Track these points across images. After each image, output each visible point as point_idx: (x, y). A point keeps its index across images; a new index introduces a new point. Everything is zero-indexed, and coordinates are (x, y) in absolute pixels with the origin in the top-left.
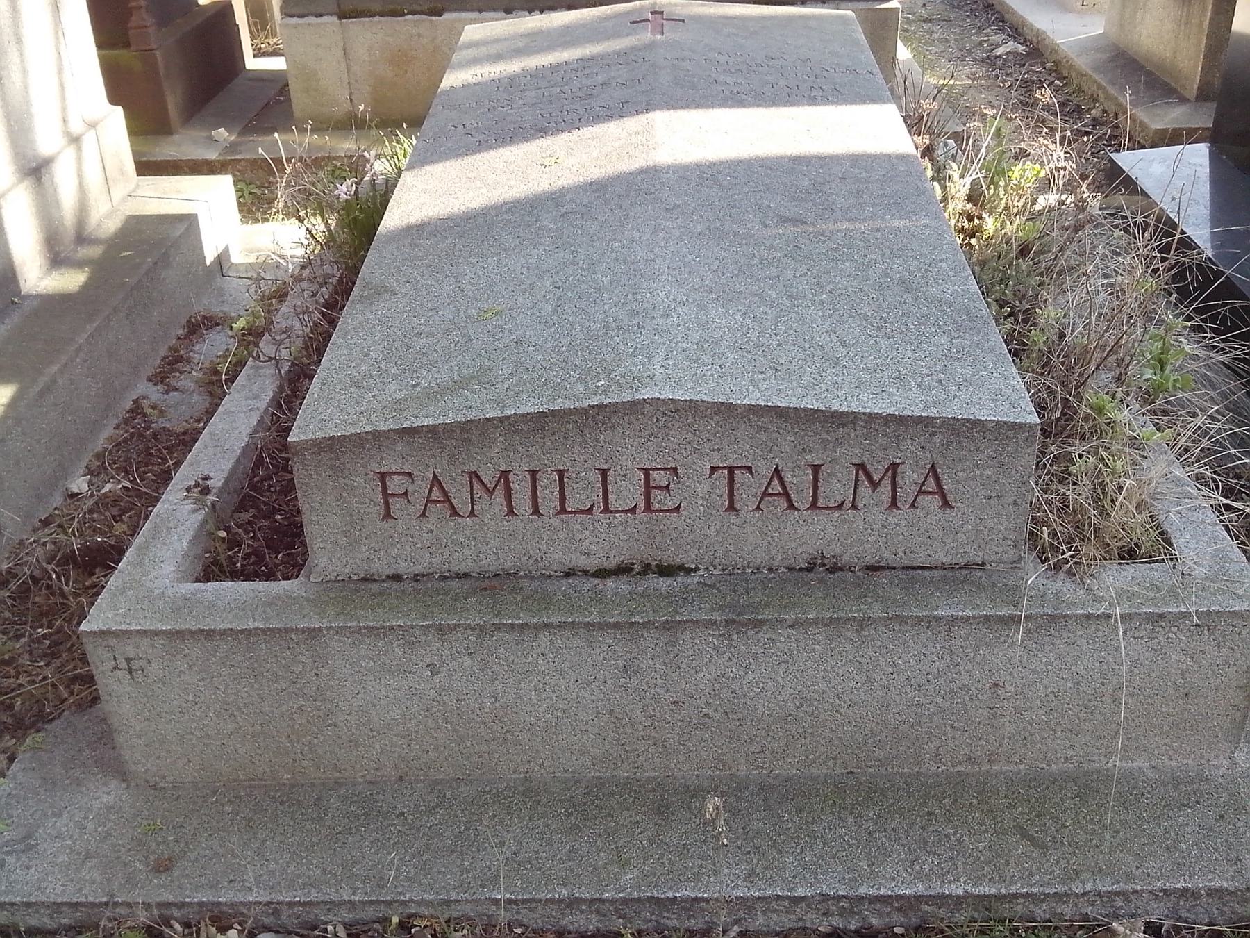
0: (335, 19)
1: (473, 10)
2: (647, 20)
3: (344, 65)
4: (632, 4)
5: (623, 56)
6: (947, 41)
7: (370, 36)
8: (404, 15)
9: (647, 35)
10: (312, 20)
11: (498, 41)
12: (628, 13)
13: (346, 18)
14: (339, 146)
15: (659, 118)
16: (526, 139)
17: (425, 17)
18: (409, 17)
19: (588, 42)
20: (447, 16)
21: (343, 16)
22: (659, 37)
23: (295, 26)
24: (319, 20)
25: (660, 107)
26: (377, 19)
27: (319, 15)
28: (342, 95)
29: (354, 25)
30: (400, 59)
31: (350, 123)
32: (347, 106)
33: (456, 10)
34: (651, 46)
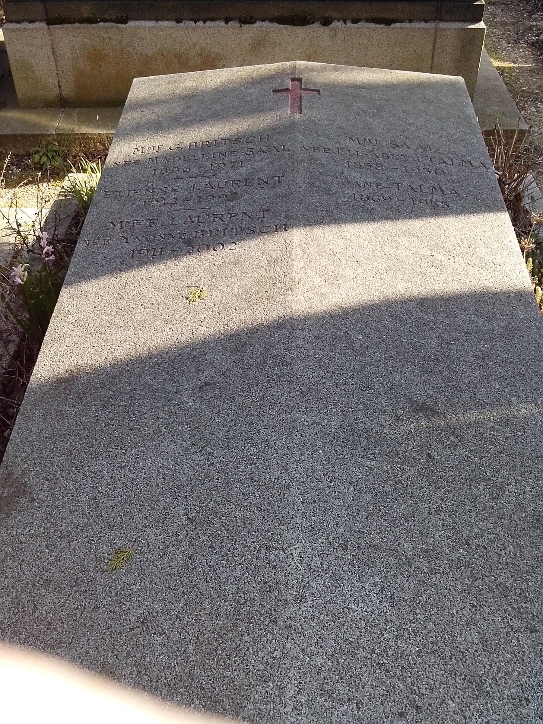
0: (43, 25)
1: (150, 19)
2: (287, 90)
3: (53, 59)
4: (276, 65)
5: (265, 135)
6: (506, 24)
7: (72, 39)
8: (97, 22)
9: (285, 113)
10: (26, 25)
11: (159, 102)
12: (271, 78)
13: (52, 24)
14: (51, 124)
15: (297, 236)
16: (175, 254)
17: (114, 24)
18: (102, 24)
19: (237, 115)
20: (132, 24)
21: (50, 23)
22: (297, 116)
23: (14, 30)
24: (32, 26)
25: (298, 226)
26: (77, 25)
27: (31, 22)
28: (52, 82)
29: (59, 30)
30: (96, 56)
31: (62, 104)
32: (56, 92)
33: (136, 19)
34: (289, 128)
